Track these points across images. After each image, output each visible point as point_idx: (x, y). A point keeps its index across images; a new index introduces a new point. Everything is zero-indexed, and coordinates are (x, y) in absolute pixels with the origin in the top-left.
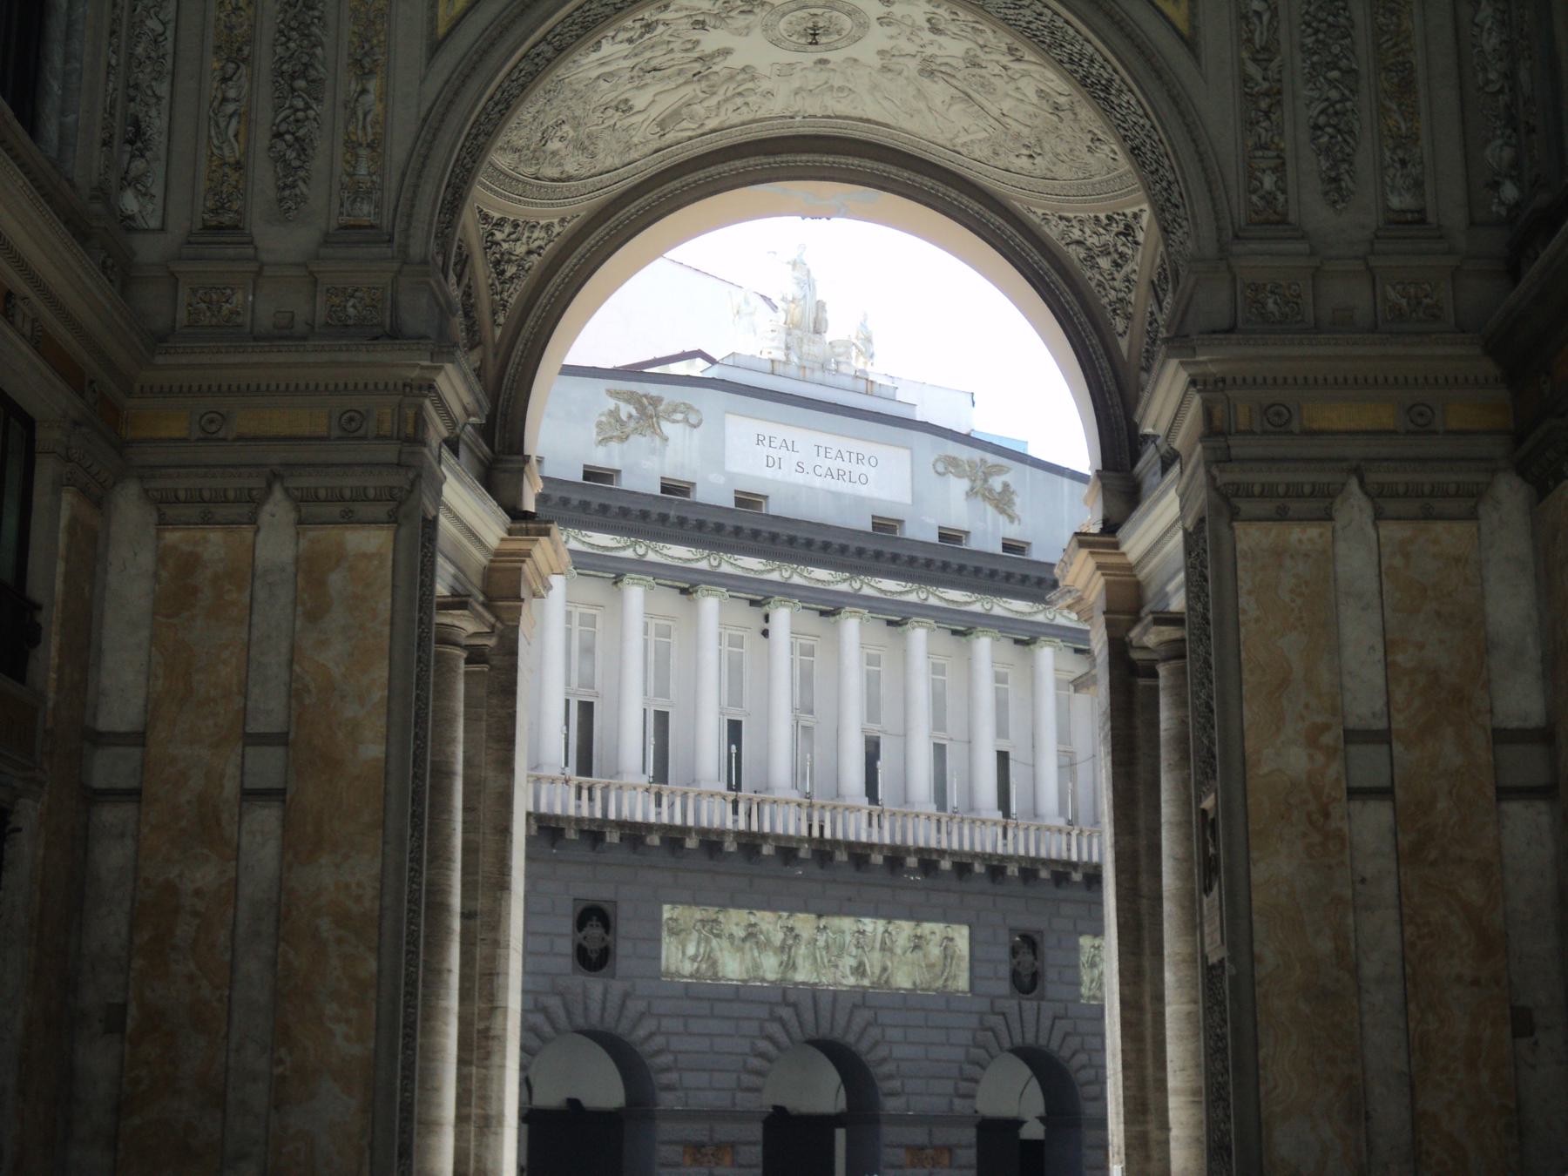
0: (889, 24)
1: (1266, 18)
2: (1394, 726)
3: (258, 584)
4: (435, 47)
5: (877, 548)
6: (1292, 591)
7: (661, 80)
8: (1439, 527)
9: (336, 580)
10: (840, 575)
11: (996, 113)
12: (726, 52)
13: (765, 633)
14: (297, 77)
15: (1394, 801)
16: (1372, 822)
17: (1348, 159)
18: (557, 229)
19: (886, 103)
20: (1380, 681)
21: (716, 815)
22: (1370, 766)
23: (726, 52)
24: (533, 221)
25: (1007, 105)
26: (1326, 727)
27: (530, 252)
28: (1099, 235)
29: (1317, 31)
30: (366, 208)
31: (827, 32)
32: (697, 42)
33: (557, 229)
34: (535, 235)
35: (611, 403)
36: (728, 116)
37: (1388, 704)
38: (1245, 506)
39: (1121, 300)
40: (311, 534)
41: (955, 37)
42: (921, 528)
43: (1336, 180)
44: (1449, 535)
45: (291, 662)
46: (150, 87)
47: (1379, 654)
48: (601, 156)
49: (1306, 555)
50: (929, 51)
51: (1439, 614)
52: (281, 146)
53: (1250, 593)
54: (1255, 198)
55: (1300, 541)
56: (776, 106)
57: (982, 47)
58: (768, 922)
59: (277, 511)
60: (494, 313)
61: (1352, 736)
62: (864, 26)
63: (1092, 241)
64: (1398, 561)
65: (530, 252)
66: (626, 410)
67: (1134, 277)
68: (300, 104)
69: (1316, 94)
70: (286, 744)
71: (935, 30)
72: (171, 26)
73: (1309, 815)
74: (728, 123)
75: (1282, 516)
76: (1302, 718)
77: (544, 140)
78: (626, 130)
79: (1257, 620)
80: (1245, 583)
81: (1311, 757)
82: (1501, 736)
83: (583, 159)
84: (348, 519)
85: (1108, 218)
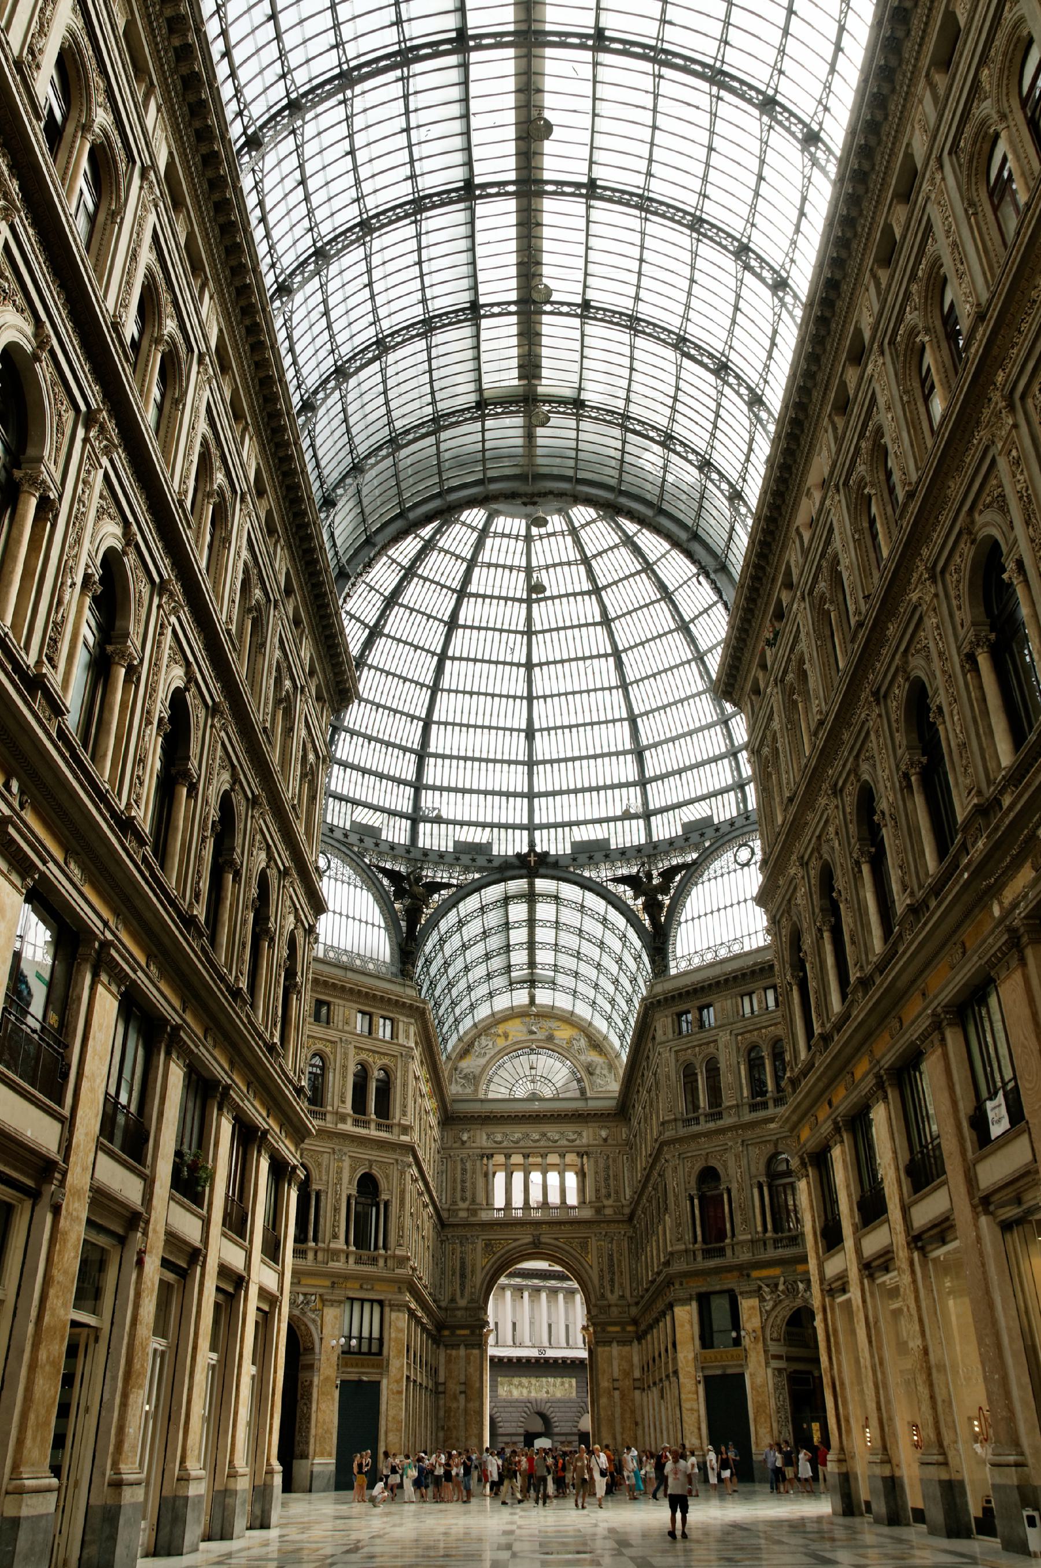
14: (463, 1276)
16: (617, 1393)
22: (616, 1384)
44: (627, 1348)
58: (524, 1380)
59: (462, 1347)
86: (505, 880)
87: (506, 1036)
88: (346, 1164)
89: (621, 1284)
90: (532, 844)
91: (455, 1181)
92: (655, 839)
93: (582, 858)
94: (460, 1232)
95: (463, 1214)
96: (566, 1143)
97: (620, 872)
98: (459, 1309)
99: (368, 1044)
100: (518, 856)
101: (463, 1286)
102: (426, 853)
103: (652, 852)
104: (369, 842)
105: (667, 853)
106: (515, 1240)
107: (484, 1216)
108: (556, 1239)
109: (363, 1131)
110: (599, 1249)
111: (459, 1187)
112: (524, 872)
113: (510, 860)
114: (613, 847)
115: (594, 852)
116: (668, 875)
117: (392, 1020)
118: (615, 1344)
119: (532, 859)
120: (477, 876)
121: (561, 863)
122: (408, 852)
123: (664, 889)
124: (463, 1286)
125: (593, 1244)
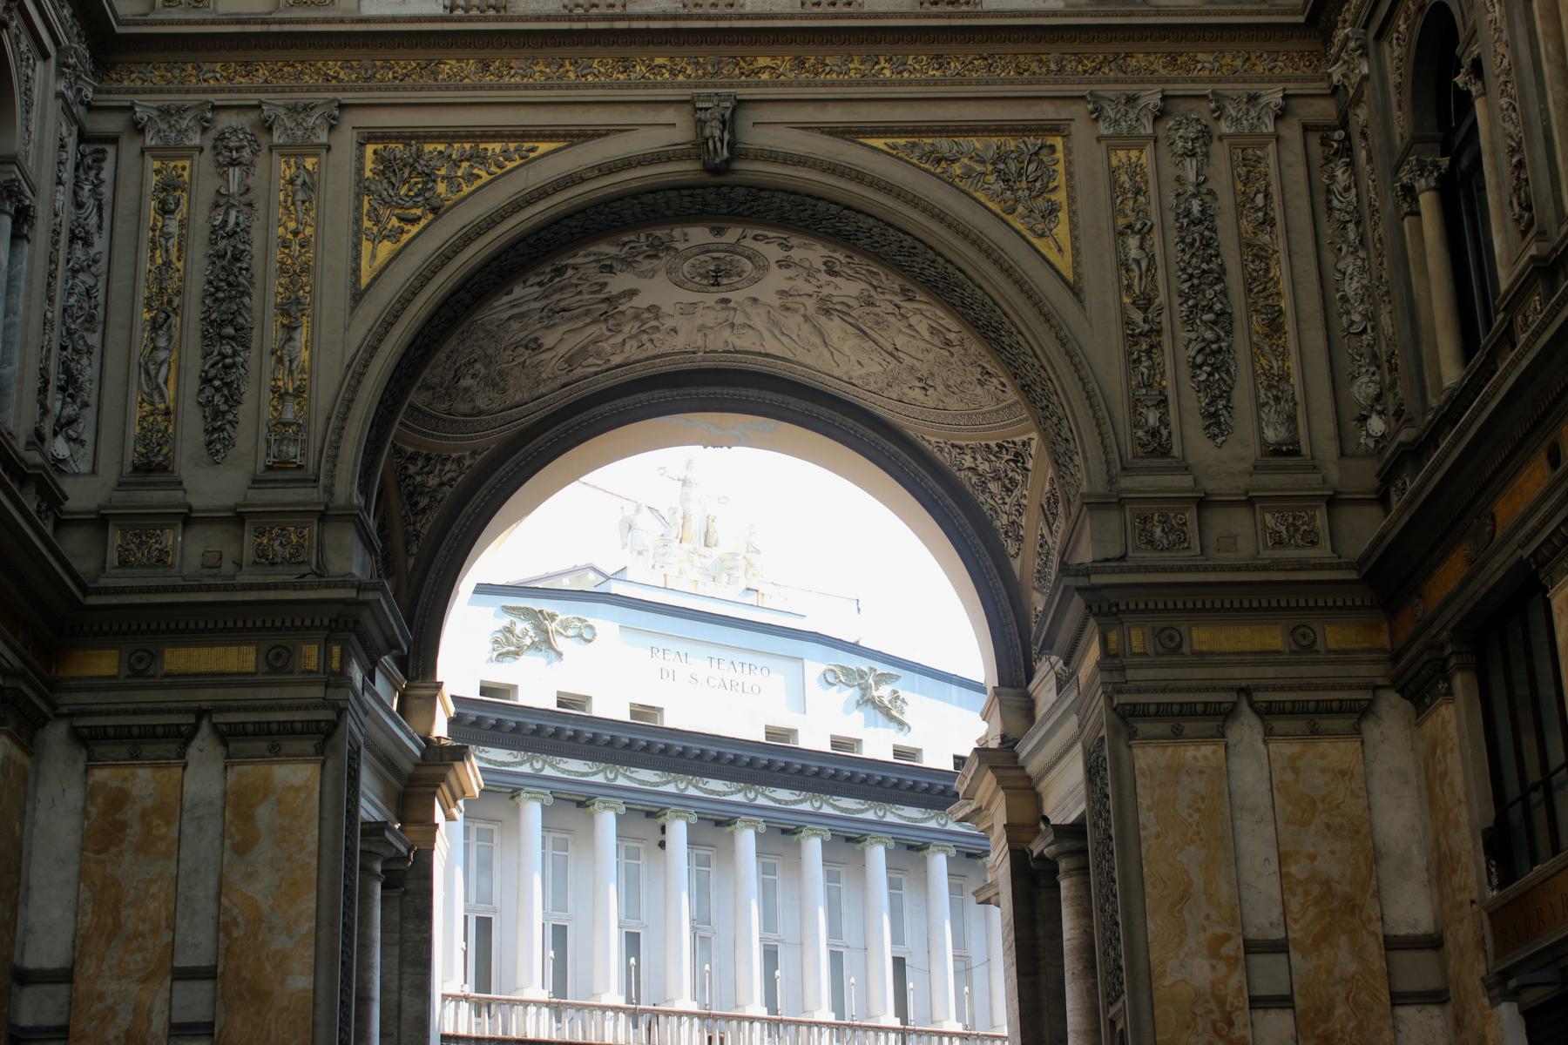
0: (788, 266)
1: (1144, 265)
2: (1291, 935)
3: (185, 817)
4: (358, 296)
5: (768, 761)
6: (1189, 807)
7: (570, 320)
8: (1325, 745)
9: (264, 813)
10: (735, 786)
11: (890, 348)
12: (632, 293)
13: (662, 845)
14: (226, 327)
15: (1293, 1008)
17: (1227, 395)
18: (467, 463)
19: (783, 339)
20: (1276, 893)
22: (1270, 975)
23: (632, 293)
24: (445, 455)
25: (900, 341)
26: (1228, 938)
27: (442, 484)
28: (990, 461)
29: (1191, 276)
30: (292, 450)
31: (728, 275)
32: (605, 285)
33: (467, 463)
34: (447, 468)
35: (506, 620)
36: (631, 351)
37: (1284, 914)
38: (1143, 727)
39: (1013, 523)
40: (238, 768)
41: (849, 278)
42: (815, 738)
43: (1215, 415)
44: (1337, 751)
45: (219, 895)
46: (82, 338)
47: (1274, 866)
48: (511, 392)
49: (1202, 772)
50: (826, 291)
51: (1328, 826)
52: (209, 391)
53: (1149, 809)
54: (1140, 433)
55: (1195, 758)
56: (680, 342)
57: (875, 288)
59: (203, 748)
60: (407, 543)
61: (1252, 947)
62: (766, 268)
63: (984, 467)
64: (1289, 776)
65: (442, 484)
66: (521, 626)
67: (1024, 501)
68: (228, 350)
69: (1193, 335)
70: (215, 978)
71: (832, 272)
72: (102, 279)
73: (1214, 1024)
74: (633, 358)
75: (1177, 735)
76: (1204, 929)
77: (457, 378)
78: (536, 366)
79: (1158, 835)
80: (1144, 800)
81: (1213, 967)
82: (1392, 944)
83: (493, 395)
84: (276, 753)
85: (1000, 446)
94: (215, 80)
98: (188, 519)
101: (221, 388)
110: (1124, 190)
118: (1246, 730)
124: (221, 388)
125: (1080, 158)
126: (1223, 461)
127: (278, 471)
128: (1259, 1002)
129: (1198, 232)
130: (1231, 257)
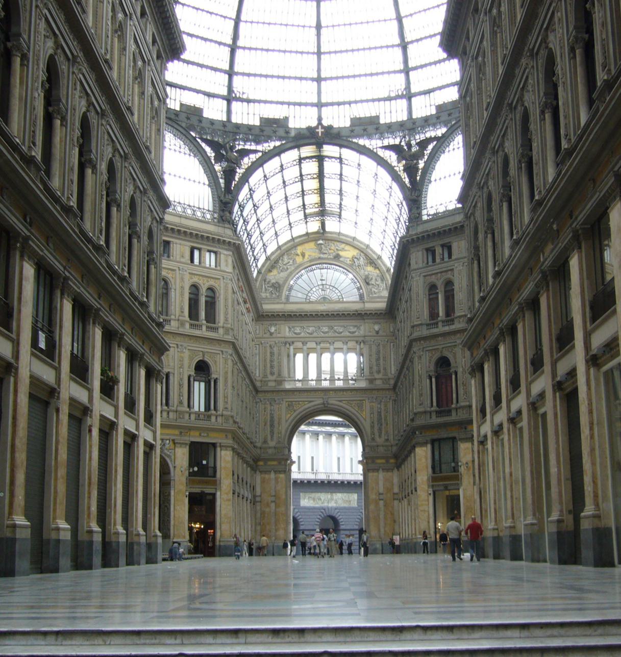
4: (286, 421)
14: (272, 426)
16: (381, 502)
21: (311, 477)
22: (381, 497)
44: (390, 474)
61: (380, 494)
82: (394, 494)
86: (298, 147)
87: (303, 255)
88: (187, 354)
89: (387, 432)
90: (320, 119)
91: (265, 360)
92: (414, 117)
93: (358, 129)
94: (269, 396)
95: (272, 384)
96: (348, 334)
97: (386, 142)
98: (270, 448)
99: (199, 271)
100: (309, 129)
101: (272, 433)
102: (238, 126)
103: (411, 126)
104: (194, 120)
105: (423, 127)
106: (311, 402)
107: (288, 386)
108: (340, 401)
109: (197, 332)
110: (372, 408)
111: (269, 365)
112: (313, 141)
113: (302, 132)
114: (382, 121)
115: (369, 126)
116: (423, 144)
117: (215, 253)
118: (381, 471)
119: (320, 130)
120: (278, 143)
121: (343, 133)
122: (224, 126)
123: (419, 155)
124: (272, 433)
125: (367, 405)
126: (380, 441)
127: (279, 442)
128: (380, 500)
129: (379, 413)
130: (383, 417)
